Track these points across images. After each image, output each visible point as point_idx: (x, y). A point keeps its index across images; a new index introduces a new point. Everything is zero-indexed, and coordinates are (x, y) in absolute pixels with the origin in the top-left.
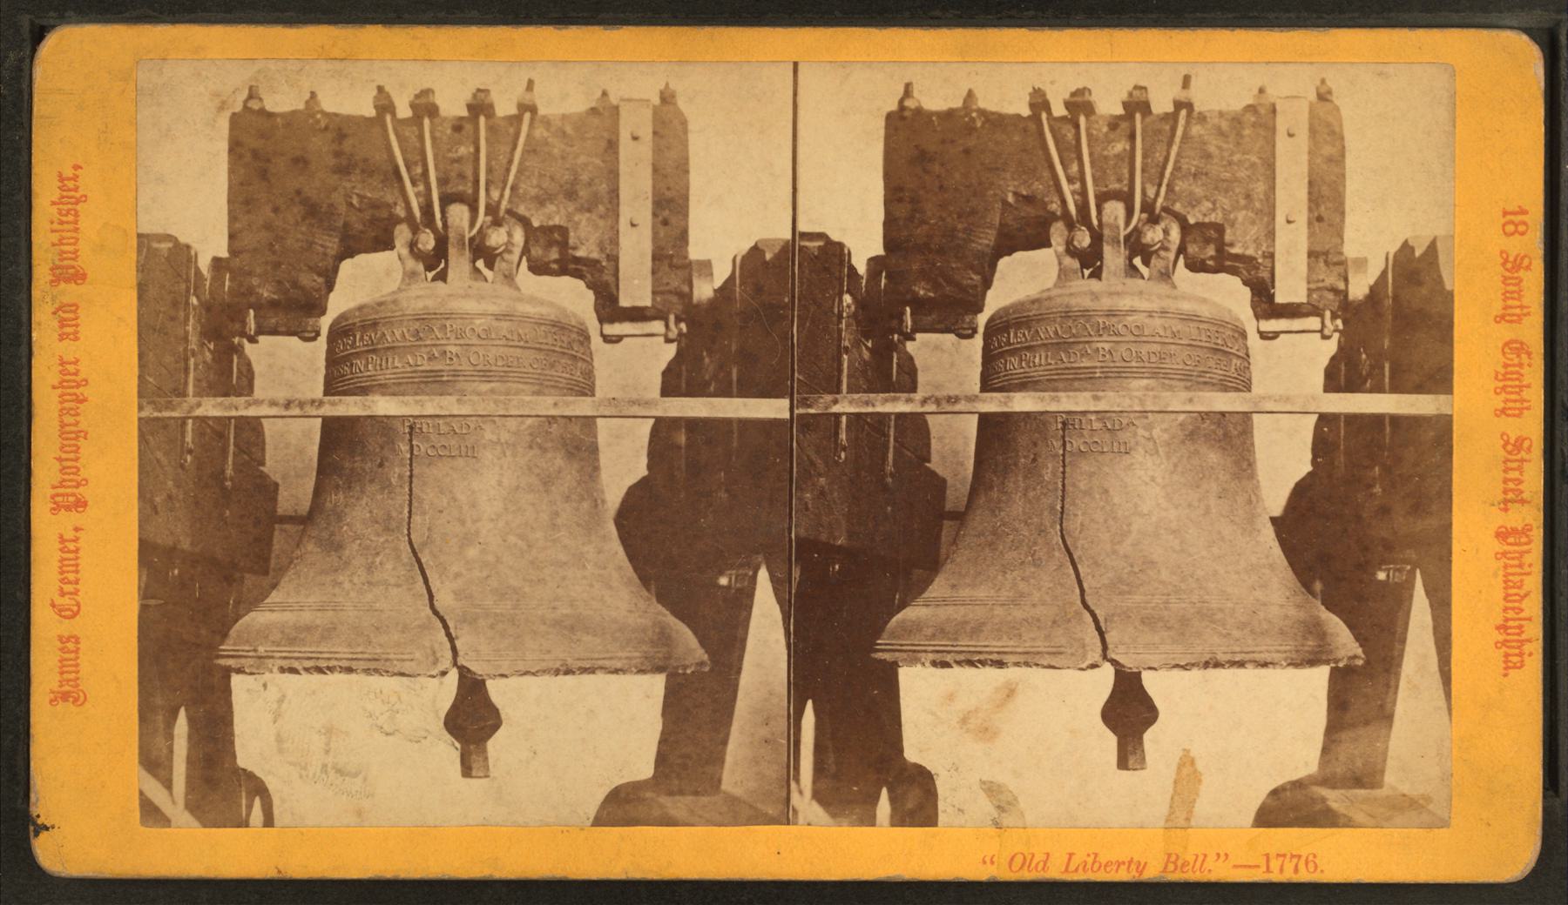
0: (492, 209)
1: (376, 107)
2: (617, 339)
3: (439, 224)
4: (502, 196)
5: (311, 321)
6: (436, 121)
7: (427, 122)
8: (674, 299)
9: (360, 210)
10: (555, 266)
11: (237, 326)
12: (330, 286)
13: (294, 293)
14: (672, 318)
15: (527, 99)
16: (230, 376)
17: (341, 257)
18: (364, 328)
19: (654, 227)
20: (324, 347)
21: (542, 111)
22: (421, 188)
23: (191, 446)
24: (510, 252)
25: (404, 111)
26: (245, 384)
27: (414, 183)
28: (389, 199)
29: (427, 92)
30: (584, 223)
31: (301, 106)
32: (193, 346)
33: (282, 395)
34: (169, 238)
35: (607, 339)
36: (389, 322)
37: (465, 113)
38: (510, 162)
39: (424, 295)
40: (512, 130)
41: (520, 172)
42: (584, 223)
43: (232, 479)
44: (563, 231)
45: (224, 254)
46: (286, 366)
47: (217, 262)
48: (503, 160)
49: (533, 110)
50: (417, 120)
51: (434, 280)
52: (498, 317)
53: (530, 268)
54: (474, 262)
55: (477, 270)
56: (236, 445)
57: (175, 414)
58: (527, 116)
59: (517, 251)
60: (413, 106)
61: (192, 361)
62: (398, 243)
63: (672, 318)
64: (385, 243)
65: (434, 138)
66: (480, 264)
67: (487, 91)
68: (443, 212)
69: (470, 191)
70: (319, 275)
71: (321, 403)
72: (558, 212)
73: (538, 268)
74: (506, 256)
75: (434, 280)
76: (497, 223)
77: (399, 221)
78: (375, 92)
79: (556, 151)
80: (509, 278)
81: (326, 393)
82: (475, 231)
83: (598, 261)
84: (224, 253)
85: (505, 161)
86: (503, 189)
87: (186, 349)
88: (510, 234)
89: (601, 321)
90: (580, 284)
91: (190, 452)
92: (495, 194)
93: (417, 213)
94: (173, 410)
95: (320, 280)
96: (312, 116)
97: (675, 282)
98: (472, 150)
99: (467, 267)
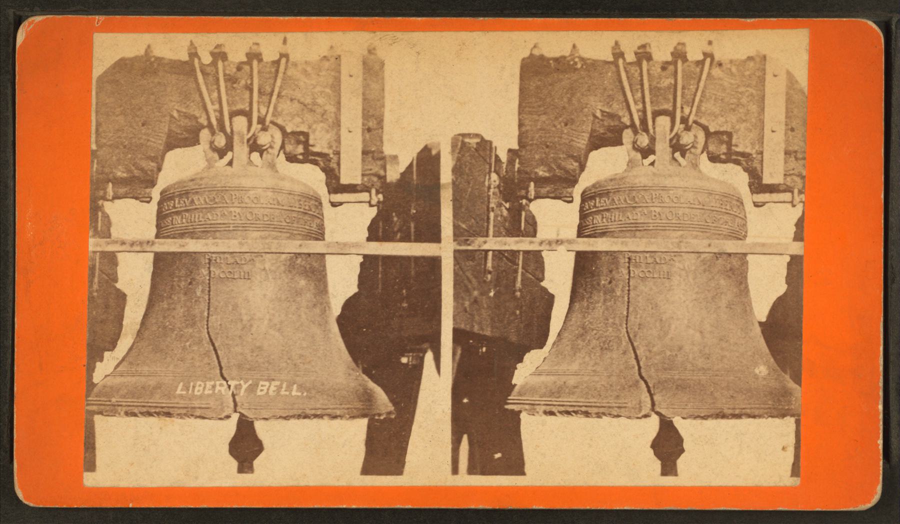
0: (684, 120)
1: (613, 54)
2: (763, 204)
4: (691, 112)
6: (651, 63)
7: (645, 63)
9: (602, 120)
10: (723, 157)
11: (523, 192)
13: (558, 172)
14: (796, 191)
15: (708, 49)
16: (520, 224)
17: (591, 150)
18: (180, 196)
19: (786, 134)
20: (156, 207)
21: (717, 57)
22: (640, 106)
23: (490, 269)
24: (693, 147)
25: (630, 57)
26: (532, 230)
27: (636, 103)
28: (621, 114)
29: (643, 46)
30: (742, 129)
31: (567, 53)
32: (492, 205)
33: (553, 236)
34: (477, 135)
35: (756, 205)
36: (618, 191)
37: (669, 58)
38: (697, 90)
39: (643, 174)
40: (698, 70)
41: (703, 95)
42: (742, 129)
43: (520, 290)
44: (730, 135)
45: (515, 146)
46: (555, 218)
47: (510, 151)
48: (693, 88)
49: (712, 56)
50: (639, 63)
52: (685, 189)
54: (673, 154)
55: (674, 159)
56: (523, 268)
57: (470, 248)
58: (708, 60)
59: (700, 146)
60: (636, 54)
61: (492, 215)
62: (624, 141)
63: (796, 191)
64: (618, 142)
65: (649, 74)
66: (677, 155)
67: (684, 44)
68: (654, 122)
69: (671, 109)
70: (576, 161)
71: (153, 243)
72: (726, 122)
73: (714, 159)
74: (693, 150)
76: (688, 129)
77: (627, 127)
78: (613, 44)
79: (726, 84)
80: (695, 166)
81: (580, 235)
82: (673, 134)
84: (515, 146)
85: (694, 90)
86: (692, 107)
87: (488, 207)
88: (696, 137)
89: (752, 192)
90: (739, 168)
91: (490, 272)
92: (687, 110)
93: (637, 122)
94: (469, 245)
95: (576, 164)
96: (573, 60)
98: (673, 82)
99: (668, 157)
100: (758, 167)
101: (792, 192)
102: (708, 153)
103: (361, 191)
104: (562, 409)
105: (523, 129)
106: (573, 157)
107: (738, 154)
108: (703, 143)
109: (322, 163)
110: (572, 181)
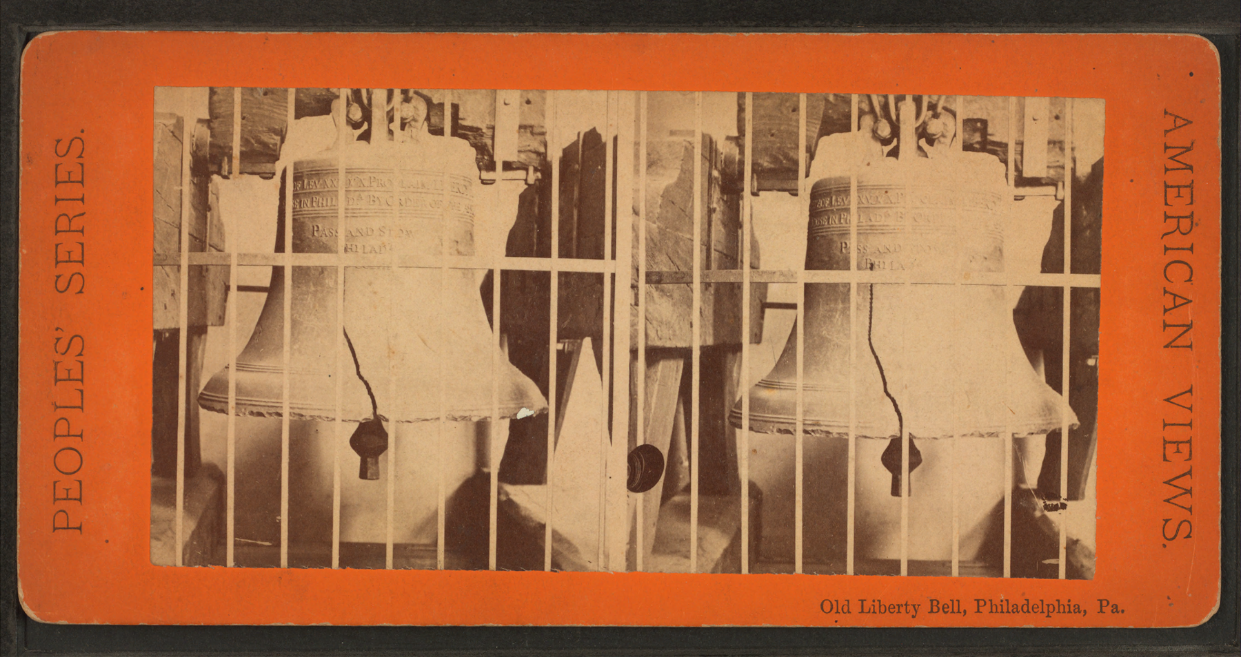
3: (365, 101)
5: (269, 166)
8: (534, 156)
12: (282, 141)
14: (531, 169)
24: (415, 120)
51: (360, 138)
53: (430, 131)
63: (531, 169)
75: (360, 138)
83: (476, 130)
89: (480, 169)
90: (466, 142)
95: (278, 138)
97: (535, 145)
100: (489, 142)
101: (527, 170)
102: (429, 125)
103: (518, 169)
104: (272, 410)
105: (215, 98)
106: (276, 132)
107: (465, 128)
108: (425, 116)
109: (473, 140)
110: (275, 158)
